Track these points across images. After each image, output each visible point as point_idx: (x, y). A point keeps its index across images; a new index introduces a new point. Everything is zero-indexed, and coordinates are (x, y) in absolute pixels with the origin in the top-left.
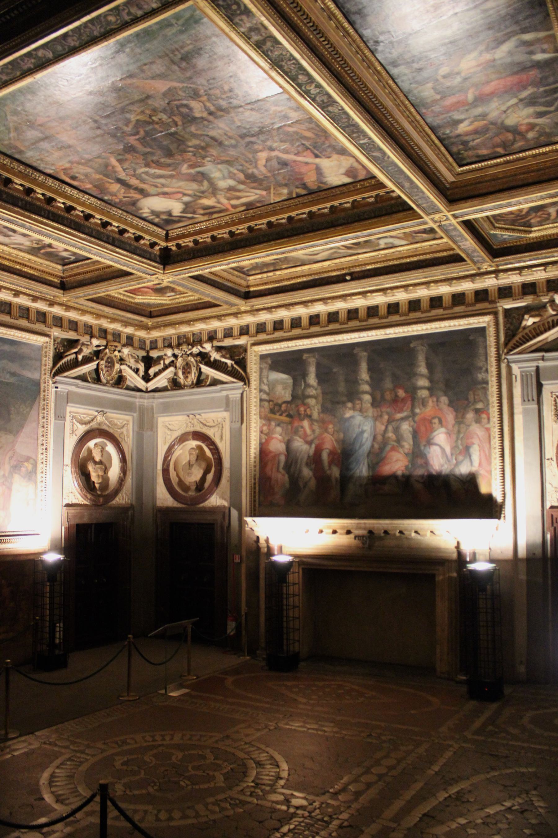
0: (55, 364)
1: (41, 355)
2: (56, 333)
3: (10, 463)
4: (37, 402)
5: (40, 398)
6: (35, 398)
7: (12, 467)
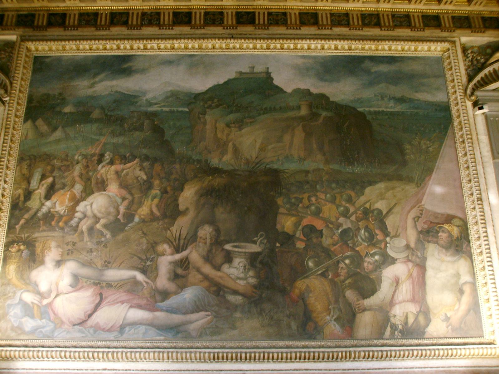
0: (470, 79)
1: (443, 69)
2: (467, 38)
3: (415, 226)
4: (450, 132)
5: (453, 126)
6: (446, 128)
7: (421, 232)
